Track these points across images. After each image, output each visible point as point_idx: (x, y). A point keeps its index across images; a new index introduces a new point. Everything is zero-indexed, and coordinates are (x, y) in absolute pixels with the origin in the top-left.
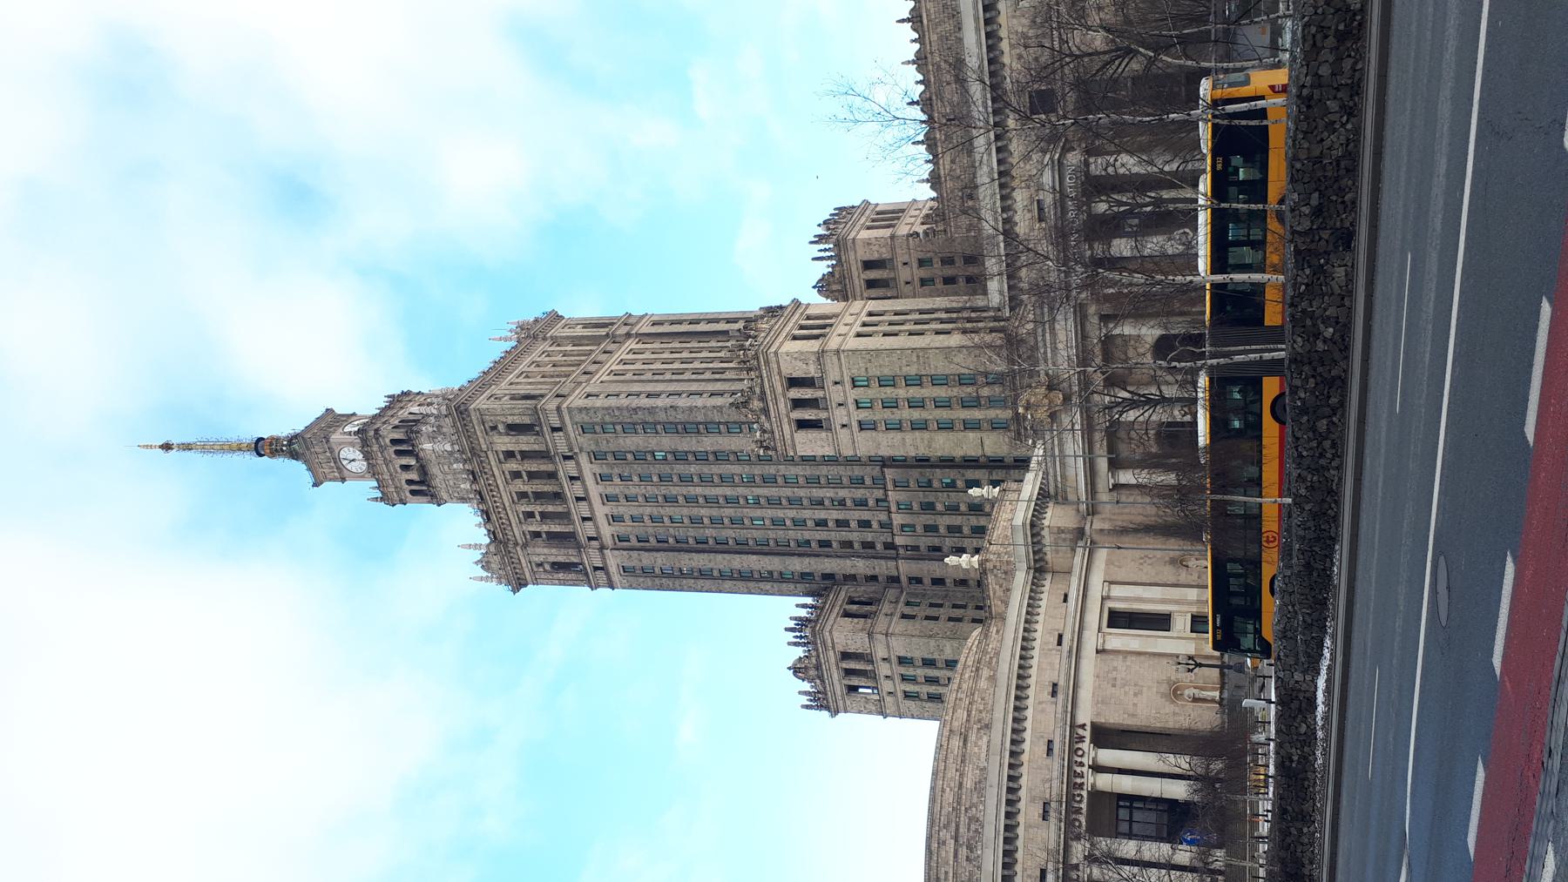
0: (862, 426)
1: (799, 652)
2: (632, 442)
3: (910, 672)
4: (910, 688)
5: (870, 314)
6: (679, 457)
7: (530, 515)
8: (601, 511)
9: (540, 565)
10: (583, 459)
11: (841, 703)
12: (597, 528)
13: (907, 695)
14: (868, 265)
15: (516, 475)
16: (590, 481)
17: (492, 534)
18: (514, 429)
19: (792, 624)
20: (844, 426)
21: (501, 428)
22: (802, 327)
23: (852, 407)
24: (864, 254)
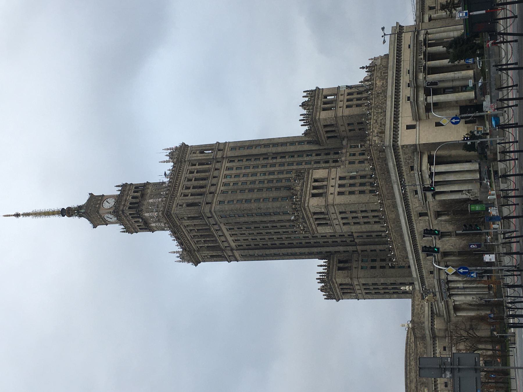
0: (344, 224)
1: (323, 284)
2: (242, 219)
3: (368, 287)
5: (341, 178)
8: (230, 239)
10: (222, 226)
11: (340, 297)
12: (229, 244)
13: (366, 293)
14: (325, 126)
17: (184, 249)
19: (318, 276)
20: (336, 225)
21: (186, 218)
22: (315, 188)
24: (323, 123)
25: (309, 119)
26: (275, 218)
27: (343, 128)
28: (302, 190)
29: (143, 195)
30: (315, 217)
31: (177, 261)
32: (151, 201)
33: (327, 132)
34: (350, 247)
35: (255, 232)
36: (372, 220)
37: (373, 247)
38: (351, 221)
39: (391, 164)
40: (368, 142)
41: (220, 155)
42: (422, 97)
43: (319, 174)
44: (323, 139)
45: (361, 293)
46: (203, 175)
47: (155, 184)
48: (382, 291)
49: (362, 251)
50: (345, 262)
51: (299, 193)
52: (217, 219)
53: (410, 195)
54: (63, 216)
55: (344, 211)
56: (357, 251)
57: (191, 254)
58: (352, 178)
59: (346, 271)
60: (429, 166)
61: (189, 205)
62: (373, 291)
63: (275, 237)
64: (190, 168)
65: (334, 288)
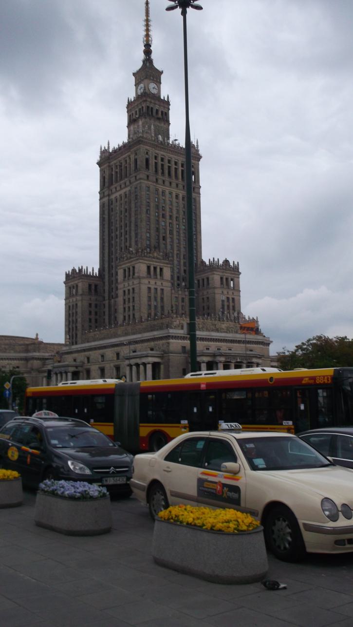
0: (124, 291)
1: (77, 271)
2: (133, 205)
3: (74, 308)
4: (71, 307)
5: (162, 290)
6: (130, 222)
8: (117, 194)
9: (104, 172)
10: (128, 189)
13: (69, 307)
14: (208, 279)
16: (124, 190)
17: (110, 154)
19: (84, 268)
21: (136, 157)
22: (155, 268)
23: (128, 288)
24: (210, 277)
25: (214, 266)
26: (133, 234)
27: (205, 293)
28: (154, 258)
29: (159, 119)
30: (131, 269)
31: (101, 147)
32: (152, 127)
33: (203, 280)
35: (122, 216)
37: (107, 313)
38: (126, 297)
39: (156, 334)
40: (175, 316)
42: (206, 359)
43: (167, 273)
45: (69, 302)
47: (168, 130)
49: (104, 305)
50: (96, 290)
51: (151, 255)
52: (134, 184)
53: (132, 347)
54: (145, 46)
55: (135, 292)
56: (104, 300)
57: (107, 159)
58: (162, 299)
59: (88, 291)
60: (151, 362)
61: (147, 160)
62: (71, 312)
63: (118, 233)
65: (74, 278)
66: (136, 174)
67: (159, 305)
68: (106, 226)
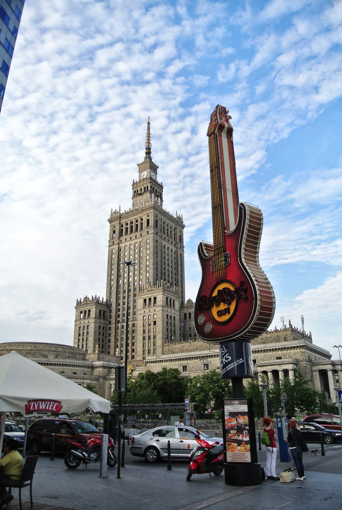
1: (91, 299)
3: (86, 328)
4: (82, 328)
5: (174, 317)
7: (127, 224)
8: (128, 244)
10: (141, 239)
13: (80, 327)
15: (137, 221)
18: (148, 221)
19: (97, 297)
21: (148, 218)
22: (170, 300)
28: (170, 292)
34: (114, 320)
36: (146, 335)
37: (113, 334)
41: (179, 246)
44: (185, 311)
46: (169, 233)
48: (81, 338)
49: (110, 328)
57: (116, 218)
58: (174, 324)
61: (157, 221)
62: (81, 332)
64: (173, 227)
66: (148, 230)
67: (173, 330)
68: (115, 267)
